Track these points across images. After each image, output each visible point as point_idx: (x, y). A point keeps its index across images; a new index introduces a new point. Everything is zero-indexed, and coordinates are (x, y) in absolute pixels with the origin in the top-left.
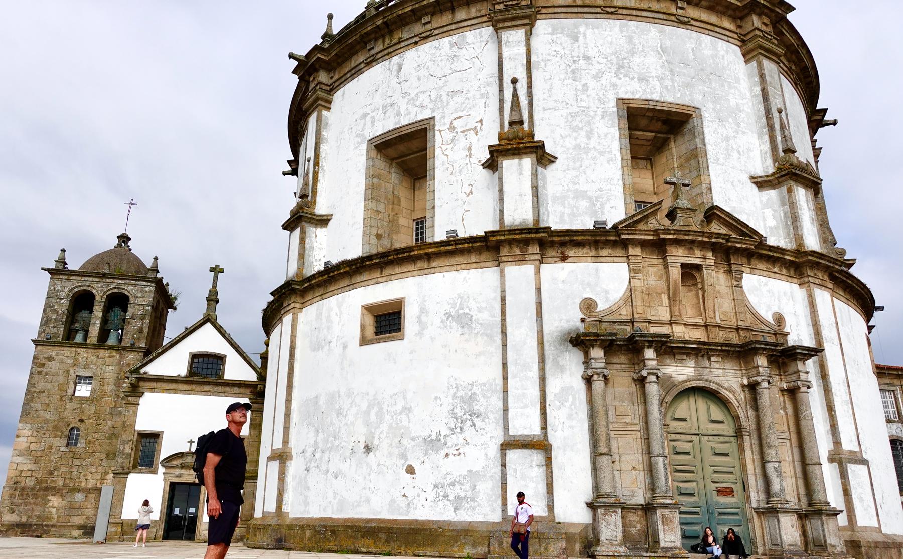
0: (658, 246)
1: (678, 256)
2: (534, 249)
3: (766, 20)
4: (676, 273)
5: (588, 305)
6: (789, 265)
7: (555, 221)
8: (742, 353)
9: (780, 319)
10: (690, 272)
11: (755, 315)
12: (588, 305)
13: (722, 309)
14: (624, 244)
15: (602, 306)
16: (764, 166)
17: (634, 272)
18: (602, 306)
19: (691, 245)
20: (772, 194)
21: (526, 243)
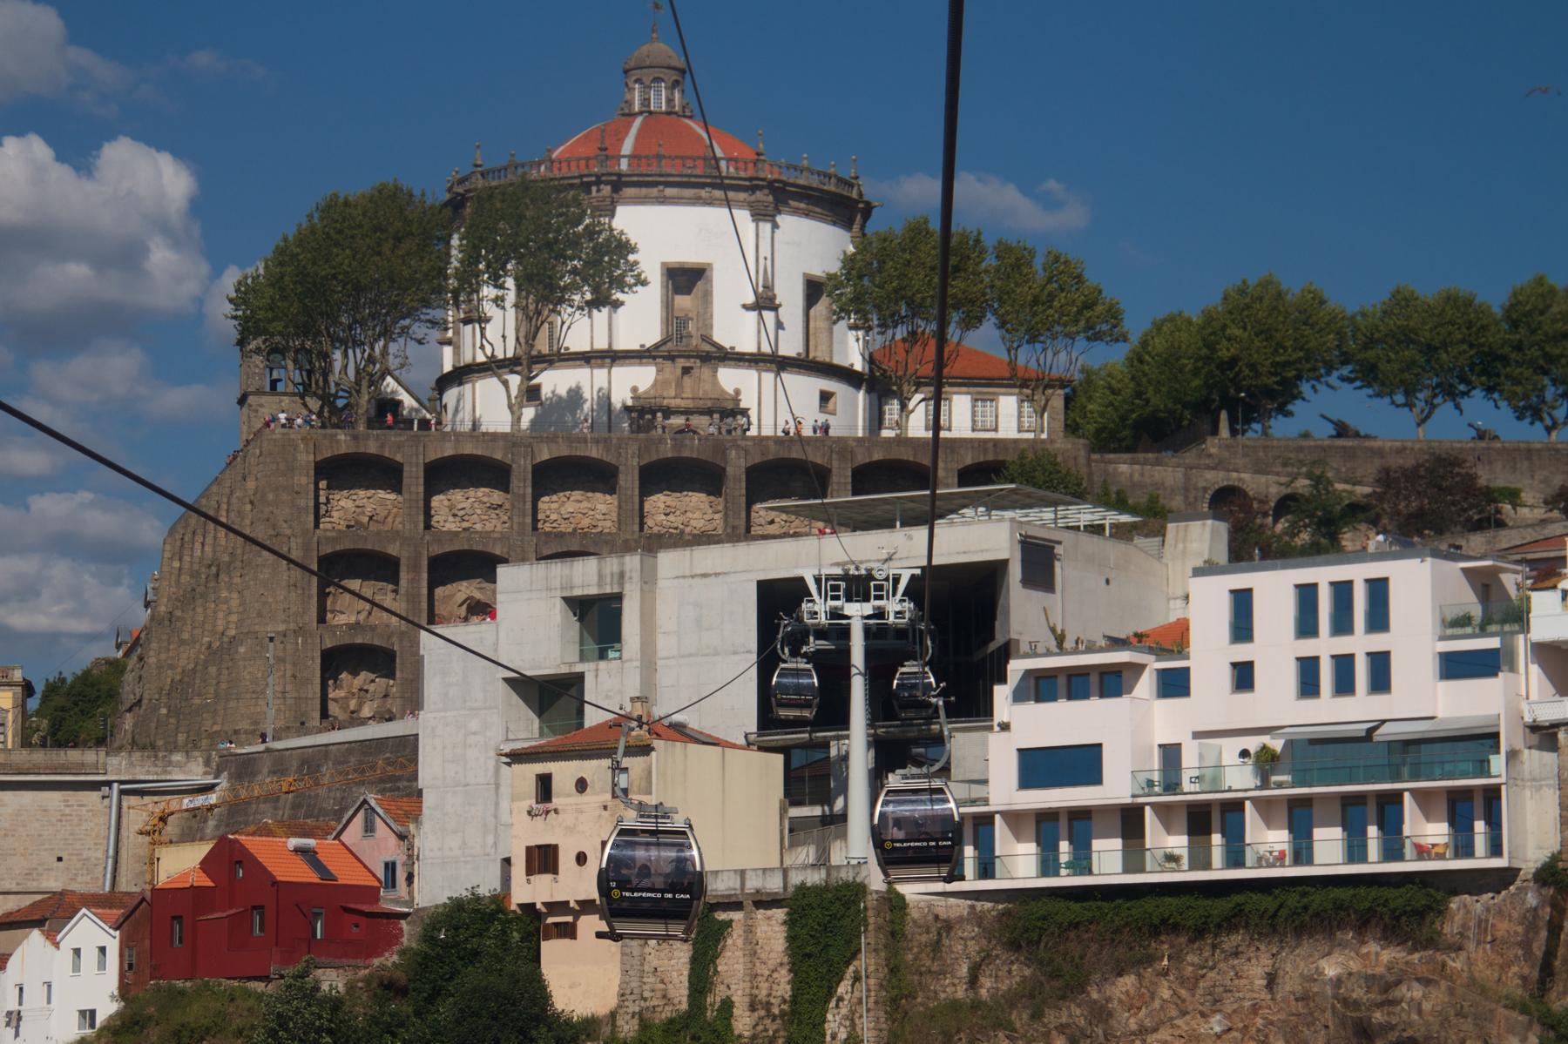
0: (671, 358)
1: (681, 362)
2: (608, 361)
3: (766, 191)
4: (679, 371)
5: (634, 389)
6: (749, 361)
7: (621, 345)
8: (709, 412)
9: (738, 392)
10: (686, 371)
11: (723, 391)
12: (634, 389)
13: (705, 388)
14: (654, 358)
15: (641, 390)
16: (750, 299)
17: (658, 371)
18: (641, 390)
19: (688, 357)
20: (753, 315)
21: (603, 358)
